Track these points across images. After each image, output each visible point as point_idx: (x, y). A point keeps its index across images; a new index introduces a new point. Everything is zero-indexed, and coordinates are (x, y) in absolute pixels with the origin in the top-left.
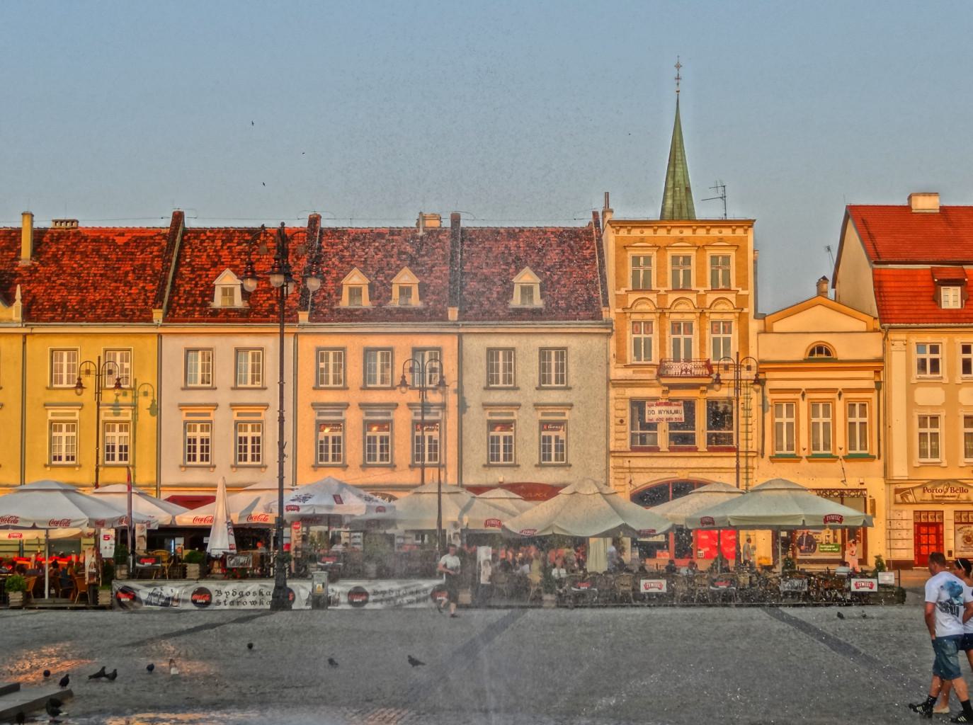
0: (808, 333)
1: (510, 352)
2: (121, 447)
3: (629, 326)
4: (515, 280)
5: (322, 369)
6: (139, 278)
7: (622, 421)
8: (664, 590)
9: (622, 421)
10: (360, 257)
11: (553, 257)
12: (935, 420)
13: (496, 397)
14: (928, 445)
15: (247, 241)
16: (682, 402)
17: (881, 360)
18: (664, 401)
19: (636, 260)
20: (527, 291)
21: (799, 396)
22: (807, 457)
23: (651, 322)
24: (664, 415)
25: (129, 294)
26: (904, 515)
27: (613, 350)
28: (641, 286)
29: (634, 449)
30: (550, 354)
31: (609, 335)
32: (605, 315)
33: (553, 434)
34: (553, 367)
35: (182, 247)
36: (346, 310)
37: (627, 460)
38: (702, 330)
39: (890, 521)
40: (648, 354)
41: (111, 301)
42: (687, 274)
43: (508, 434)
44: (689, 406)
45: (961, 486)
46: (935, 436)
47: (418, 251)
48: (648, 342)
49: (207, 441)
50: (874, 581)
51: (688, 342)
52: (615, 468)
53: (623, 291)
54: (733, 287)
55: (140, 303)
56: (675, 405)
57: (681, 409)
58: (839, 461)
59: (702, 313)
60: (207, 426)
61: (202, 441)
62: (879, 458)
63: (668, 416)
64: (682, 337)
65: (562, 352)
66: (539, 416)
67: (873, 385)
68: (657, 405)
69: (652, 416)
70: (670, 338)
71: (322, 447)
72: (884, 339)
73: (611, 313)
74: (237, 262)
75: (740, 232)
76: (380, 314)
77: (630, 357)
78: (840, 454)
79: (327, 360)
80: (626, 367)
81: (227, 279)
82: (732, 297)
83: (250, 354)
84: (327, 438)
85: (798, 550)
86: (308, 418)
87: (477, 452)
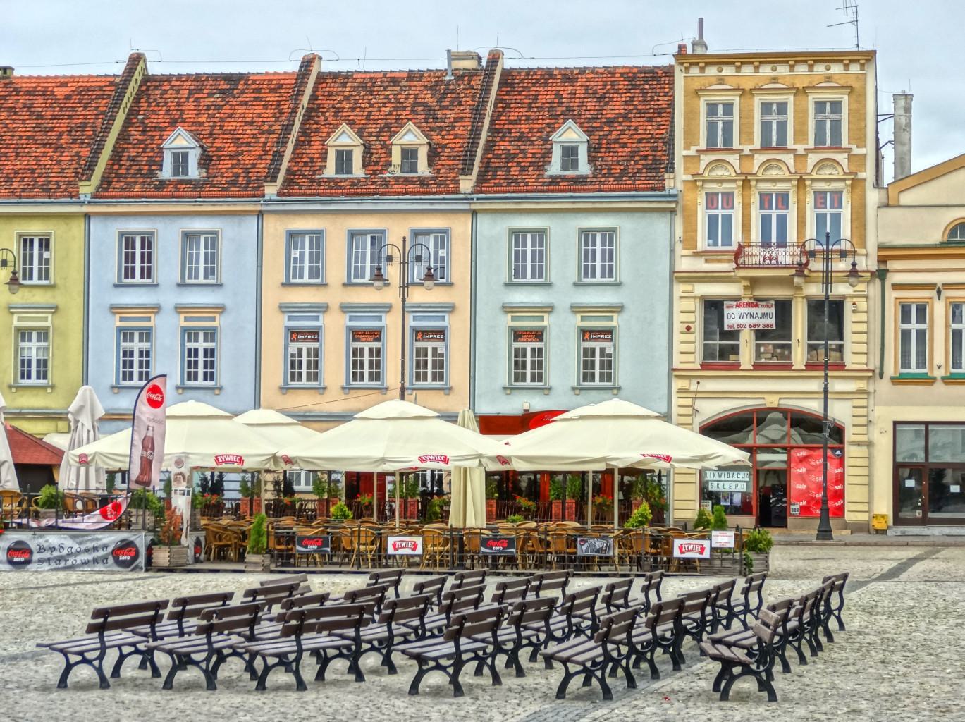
0: (947, 206)
1: (540, 235)
2: (39, 361)
3: (702, 200)
5: (295, 259)
6: (74, 141)
7: (688, 328)
8: (419, 551)
9: (688, 328)
10: (363, 109)
11: (616, 108)
13: (520, 297)
15: (222, 92)
16: (773, 302)
18: (746, 300)
19: (712, 109)
20: (570, 153)
21: (934, 293)
22: (943, 378)
25: (59, 162)
27: (679, 231)
28: (720, 141)
30: (594, 238)
31: (672, 211)
32: (669, 184)
34: (598, 257)
35: (137, 100)
36: (330, 180)
37: (695, 381)
40: (728, 239)
41: (33, 171)
44: (783, 309)
47: (440, 101)
48: (728, 219)
49: (148, 354)
50: (706, 543)
51: (782, 221)
53: (692, 152)
54: (845, 144)
55: (69, 174)
56: (763, 306)
57: (772, 311)
59: (801, 181)
60: (147, 335)
61: (141, 353)
63: (756, 321)
64: (774, 213)
66: (577, 321)
69: (731, 322)
70: (756, 214)
71: (294, 365)
73: (677, 180)
74: (203, 119)
75: (855, 68)
76: (377, 186)
77: (702, 243)
79: (303, 248)
80: (697, 254)
81: (180, 140)
82: (842, 158)
83: (307, 238)
84: (300, 350)
86: (275, 326)
87: (496, 368)
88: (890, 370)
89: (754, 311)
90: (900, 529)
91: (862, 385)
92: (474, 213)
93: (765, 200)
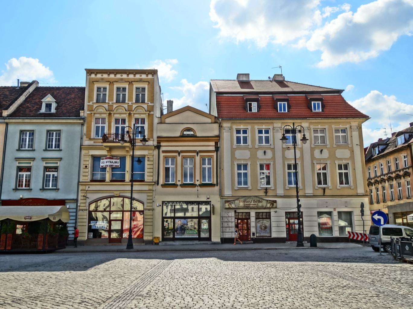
0: (182, 123)
4: (43, 100)
7: (86, 167)
9: (86, 167)
12: (245, 167)
14: (242, 179)
17: (218, 136)
18: (108, 157)
22: (180, 185)
23: (105, 119)
24: (108, 164)
26: (230, 214)
29: (92, 181)
32: (82, 114)
33: (51, 173)
34: (53, 141)
37: (87, 187)
38: (130, 122)
39: (222, 217)
42: (124, 96)
43: (29, 173)
44: (123, 159)
45: (259, 199)
46: (246, 175)
52: (81, 190)
53: (91, 103)
54: (146, 101)
56: (115, 159)
58: (197, 187)
62: (217, 186)
63: (112, 164)
64: (120, 126)
65: (59, 132)
67: (213, 148)
68: (106, 159)
72: (220, 126)
75: (150, 76)
77: (93, 134)
78: (198, 183)
80: (90, 139)
85: (176, 233)
88: (161, 181)
89: (111, 160)
90: (164, 243)
91: (151, 187)
92: (7, 124)
93: (117, 121)
